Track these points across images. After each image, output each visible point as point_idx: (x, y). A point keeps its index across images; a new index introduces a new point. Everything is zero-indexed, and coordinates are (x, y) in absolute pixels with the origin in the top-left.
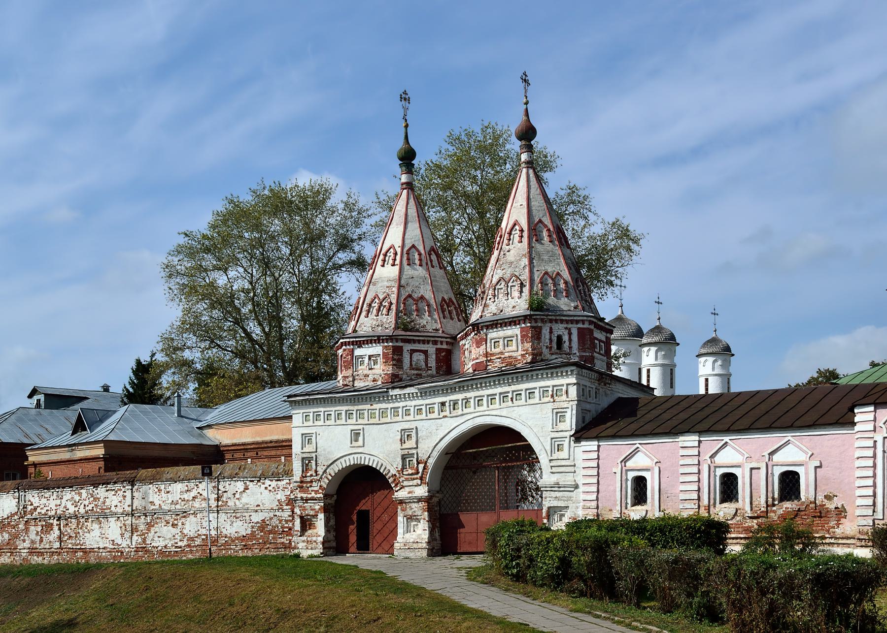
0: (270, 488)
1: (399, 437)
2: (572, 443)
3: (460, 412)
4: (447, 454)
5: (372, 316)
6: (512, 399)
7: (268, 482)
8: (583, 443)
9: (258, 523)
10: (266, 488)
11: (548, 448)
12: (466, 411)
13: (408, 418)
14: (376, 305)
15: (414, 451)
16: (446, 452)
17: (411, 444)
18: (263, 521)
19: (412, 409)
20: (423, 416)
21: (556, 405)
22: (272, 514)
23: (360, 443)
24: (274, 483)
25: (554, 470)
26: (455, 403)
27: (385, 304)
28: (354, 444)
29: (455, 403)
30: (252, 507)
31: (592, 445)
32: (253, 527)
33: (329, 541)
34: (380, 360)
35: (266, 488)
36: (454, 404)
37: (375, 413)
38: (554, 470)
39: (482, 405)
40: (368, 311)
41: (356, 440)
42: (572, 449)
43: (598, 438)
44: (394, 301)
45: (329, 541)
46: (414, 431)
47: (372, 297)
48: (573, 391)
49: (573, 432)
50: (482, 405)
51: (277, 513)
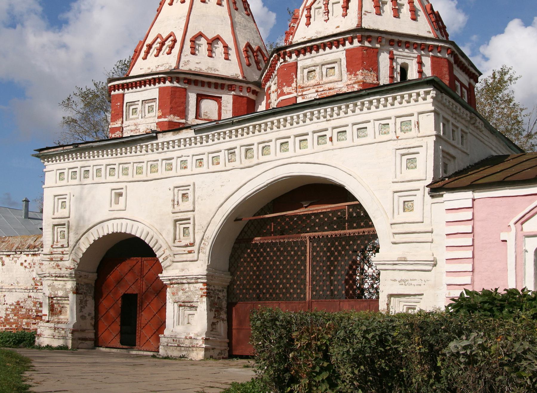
0: (26, 264)
1: (171, 198)
2: (427, 197)
3: (255, 161)
4: (236, 220)
5: (151, 56)
6: (331, 139)
7: (23, 257)
8: (447, 196)
9: (13, 304)
10: (22, 264)
11: (388, 207)
12: (262, 159)
13: (184, 172)
14: (156, 45)
15: (189, 215)
16: (235, 217)
17: (186, 205)
18: (18, 303)
19: (189, 159)
20: (204, 169)
21: (402, 144)
22: (26, 295)
23: (121, 205)
24: (30, 259)
25: (398, 238)
26: (248, 149)
27: (168, 43)
28: (115, 207)
29: (248, 149)
30: (6, 286)
31: (463, 198)
32: (7, 309)
33: (83, 331)
34: (156, 105)
35: (22, 264)
36: (247, 150)
37: (141, 168)
38: (398, 238)
39: (287, 150)
40: (147, 53)
41: (117, 203)
42: (427, 208)
43: (473, 187)
44: (179, 39)
45: (83, 331)
46: (191, 188)
47: (155, 36)
48: (429, 124)
49: (430, 181)
50: (287, 150)
51: (32, 294)
